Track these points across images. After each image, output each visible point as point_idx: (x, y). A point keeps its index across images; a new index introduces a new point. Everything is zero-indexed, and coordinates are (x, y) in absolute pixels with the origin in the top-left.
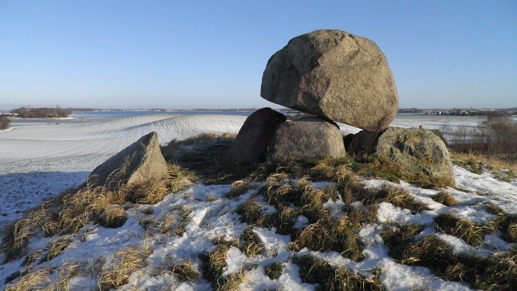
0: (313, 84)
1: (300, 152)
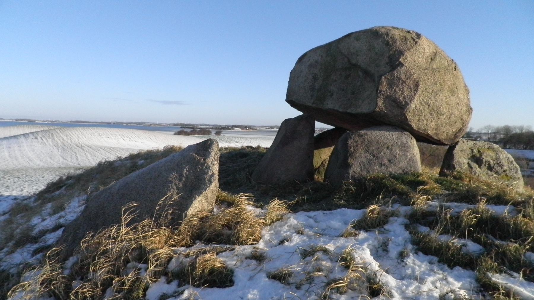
0: (397, 87)
1: (383, 168)
